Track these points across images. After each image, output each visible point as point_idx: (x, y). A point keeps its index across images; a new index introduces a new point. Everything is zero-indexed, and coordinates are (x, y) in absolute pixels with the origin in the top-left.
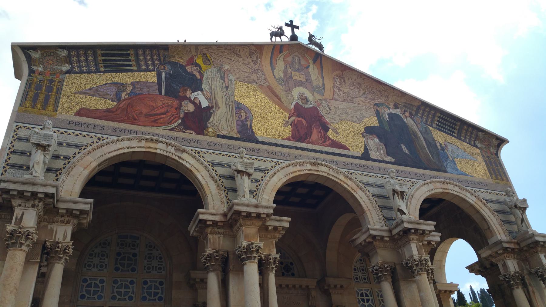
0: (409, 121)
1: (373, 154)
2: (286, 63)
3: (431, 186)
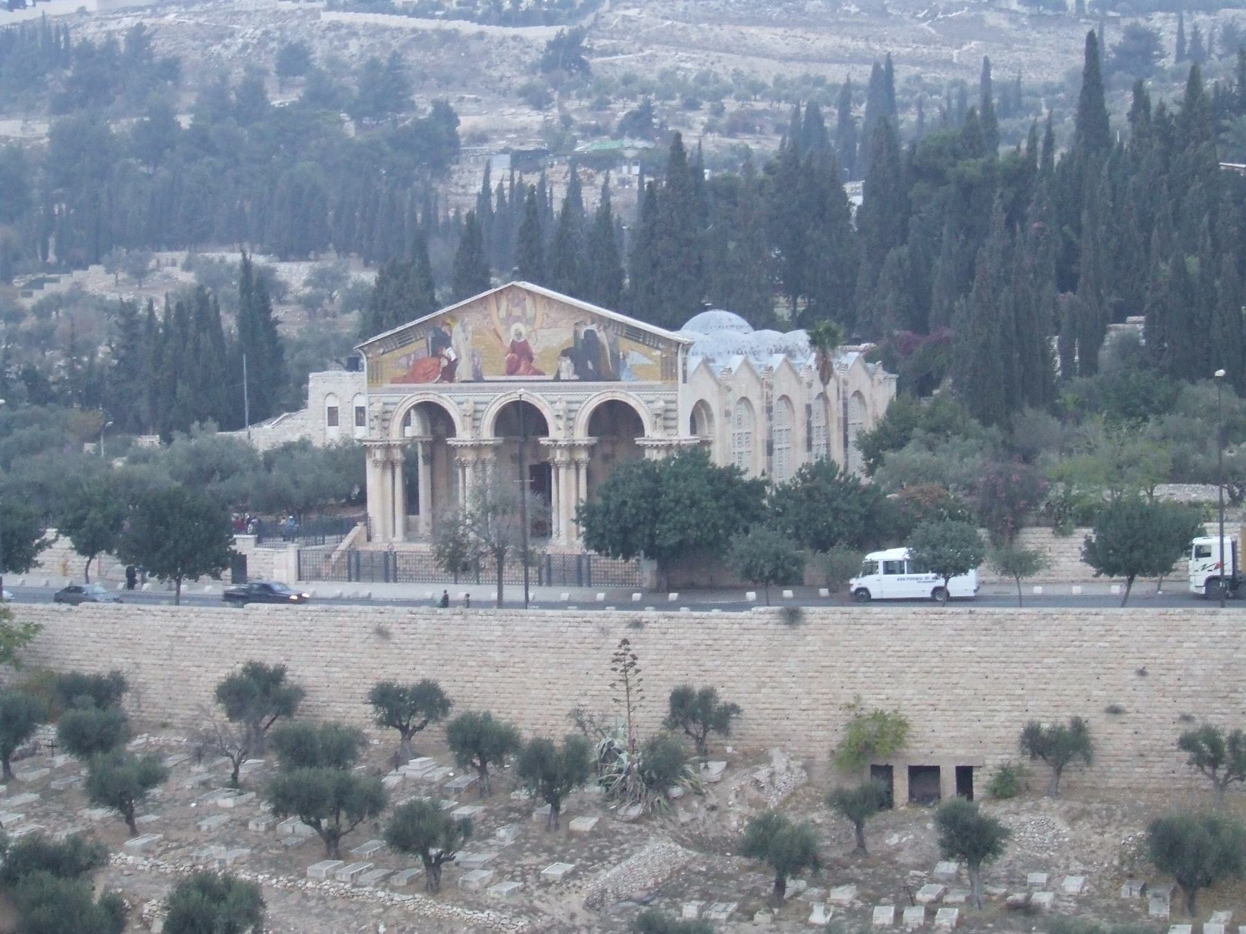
0: (601, 335)
1: (563, 376)
2: (508, 300)
3: (602, 396)
